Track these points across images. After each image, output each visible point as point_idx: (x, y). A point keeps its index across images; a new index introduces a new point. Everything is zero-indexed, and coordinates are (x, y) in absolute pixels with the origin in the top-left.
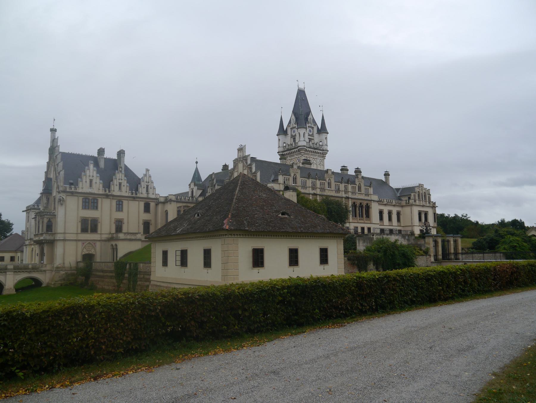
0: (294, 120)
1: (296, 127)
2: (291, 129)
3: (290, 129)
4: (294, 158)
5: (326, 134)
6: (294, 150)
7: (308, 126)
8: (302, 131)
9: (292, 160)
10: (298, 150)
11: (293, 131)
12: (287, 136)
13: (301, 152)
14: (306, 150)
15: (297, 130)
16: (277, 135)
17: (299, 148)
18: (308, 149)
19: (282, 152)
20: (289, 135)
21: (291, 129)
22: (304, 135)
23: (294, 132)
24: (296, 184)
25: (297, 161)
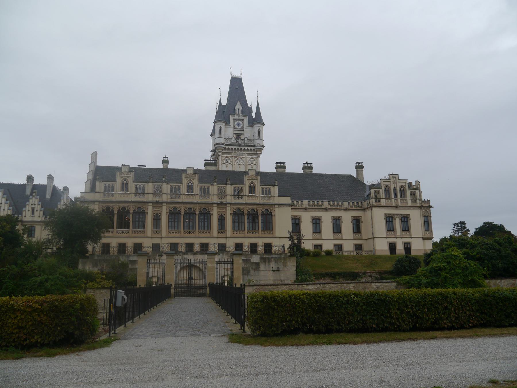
1: (243, 120)
2: (234, 120)
4: (243, 157)
6: (246, 148)
10: (254, 149)
12: (229, 126)
19: (225, 145)
20: (232, 126)
25: (250, 162)
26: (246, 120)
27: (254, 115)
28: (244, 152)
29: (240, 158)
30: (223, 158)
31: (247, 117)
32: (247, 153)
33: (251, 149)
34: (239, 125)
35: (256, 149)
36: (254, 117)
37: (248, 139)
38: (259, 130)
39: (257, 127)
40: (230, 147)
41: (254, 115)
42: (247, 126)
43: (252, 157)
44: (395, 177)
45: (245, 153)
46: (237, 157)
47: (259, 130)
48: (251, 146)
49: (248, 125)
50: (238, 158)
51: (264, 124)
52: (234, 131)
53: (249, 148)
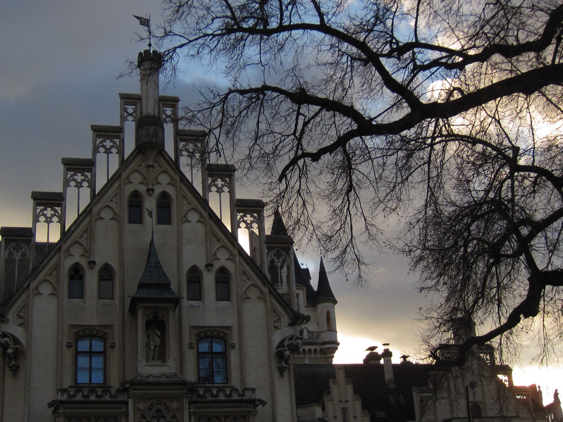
10: (321, 350)
26: (302, 294)
27: (314, 283)
31: (305, 289)
33: (315, 350)
35: (324, 349)
36: (315, 288)
37: (308, 332)
38: (328, 313)
39: (322, 307)
41: (314, 283)
42: (306, 306)
47: (328, 313)
48: (315, 344)
49: (307, 304)
51: (337, 302)
53: (312, 348)
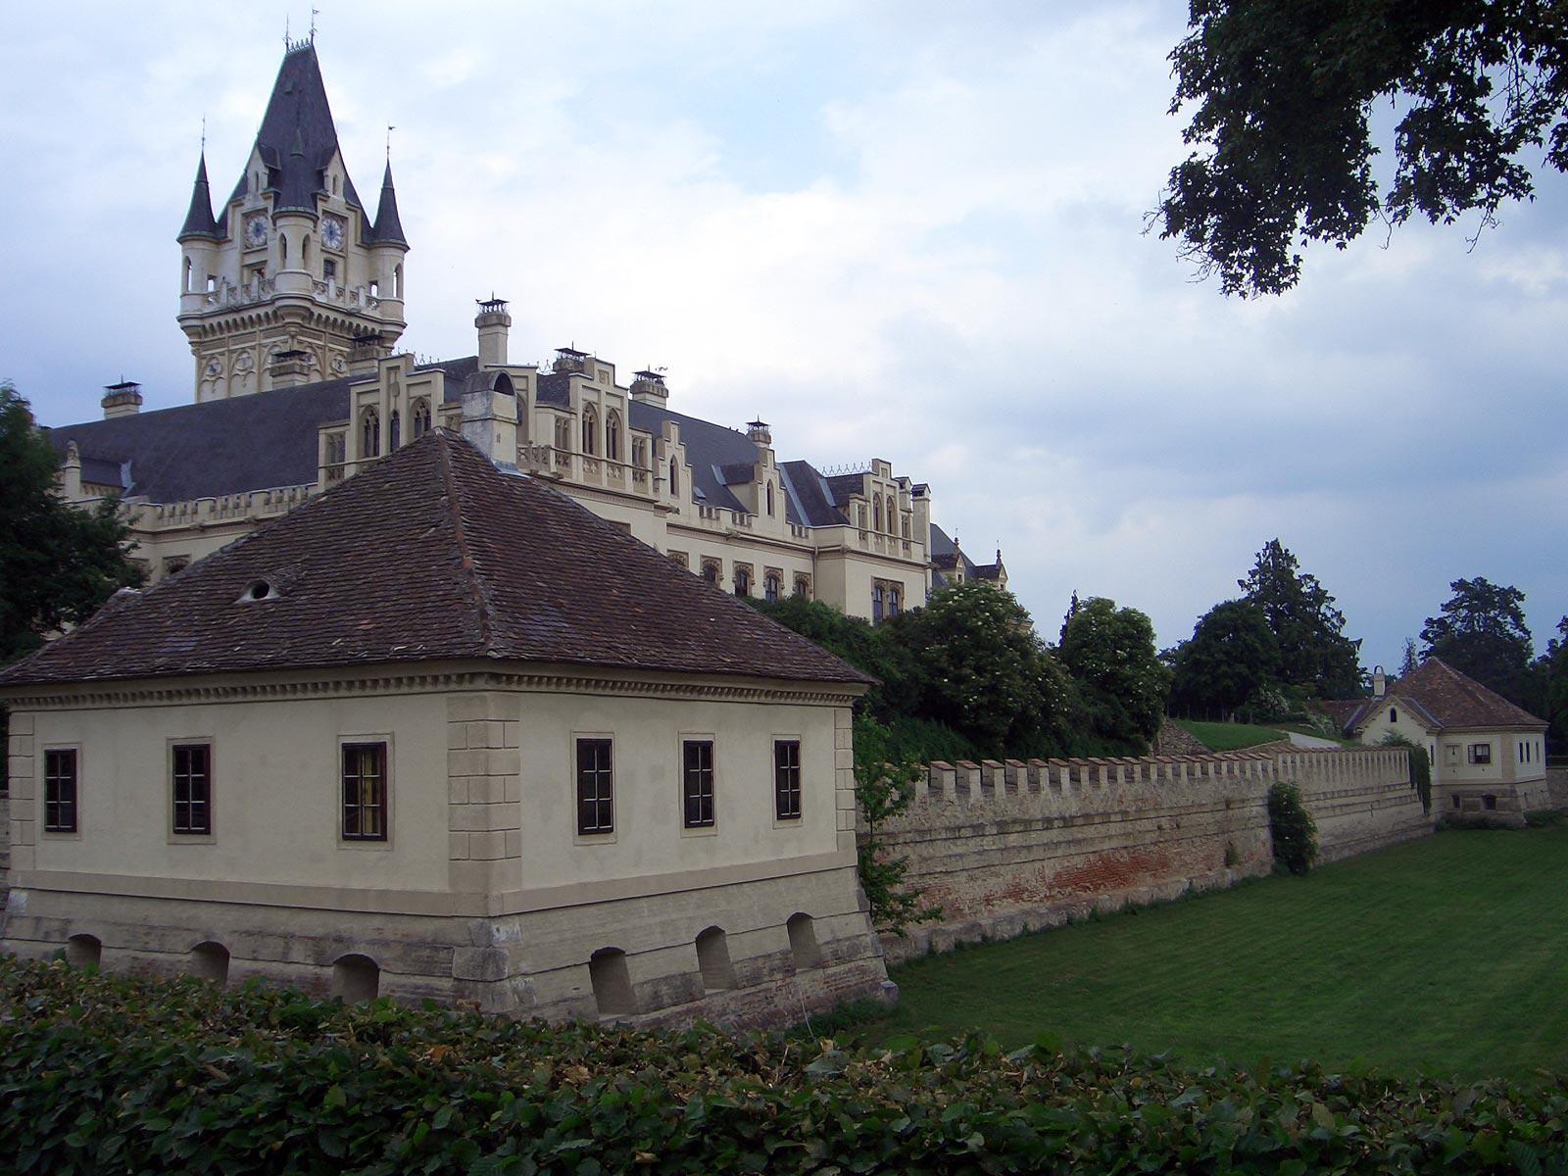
0: (264, 181)
1: (266, 210)
2: (247, 216)
3: (238, 218)
5: (399, 253)
6: (253, 313)
7: (324, 212)
8: (293, 229)
9: (245, 356)
10: (275, 313)
11: (253, 224)
12: (226, 246)
13: (287, 320)
14: (312, 314)
15: (274, 224)
16: (181, 240)
17: (279, 303)
18: (316, 311)
19: (201, 318)
21: (247, 216)
22: (304, 246)
23: (258, 230)
24: (614, 458)
28: (252, 330)
29: (244, 351)
30: (204, 362)
32: (261, 331)
34: (258, 230)
40: (214, 321)
43: (243, 346)
44: (398, 367)
45: (255, 332)
46: (234, 351)
50: (271, 349)
52: (246, 257)
53: (262, 311)
